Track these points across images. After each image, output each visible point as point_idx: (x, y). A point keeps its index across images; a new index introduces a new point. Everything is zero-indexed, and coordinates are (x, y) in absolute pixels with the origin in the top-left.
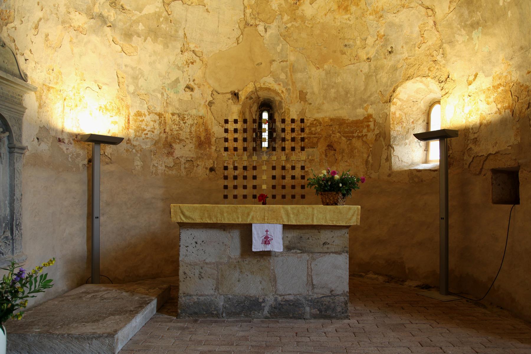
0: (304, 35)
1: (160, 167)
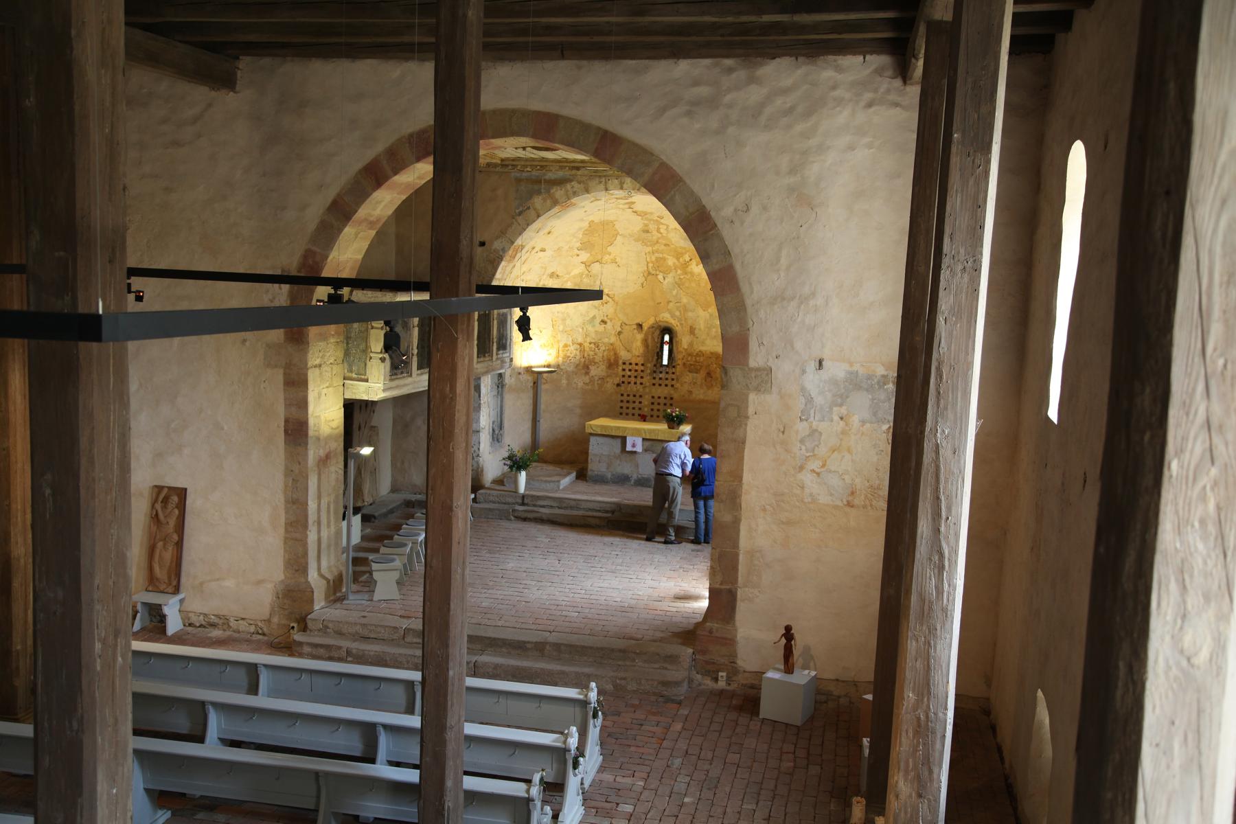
0: (693, 285)
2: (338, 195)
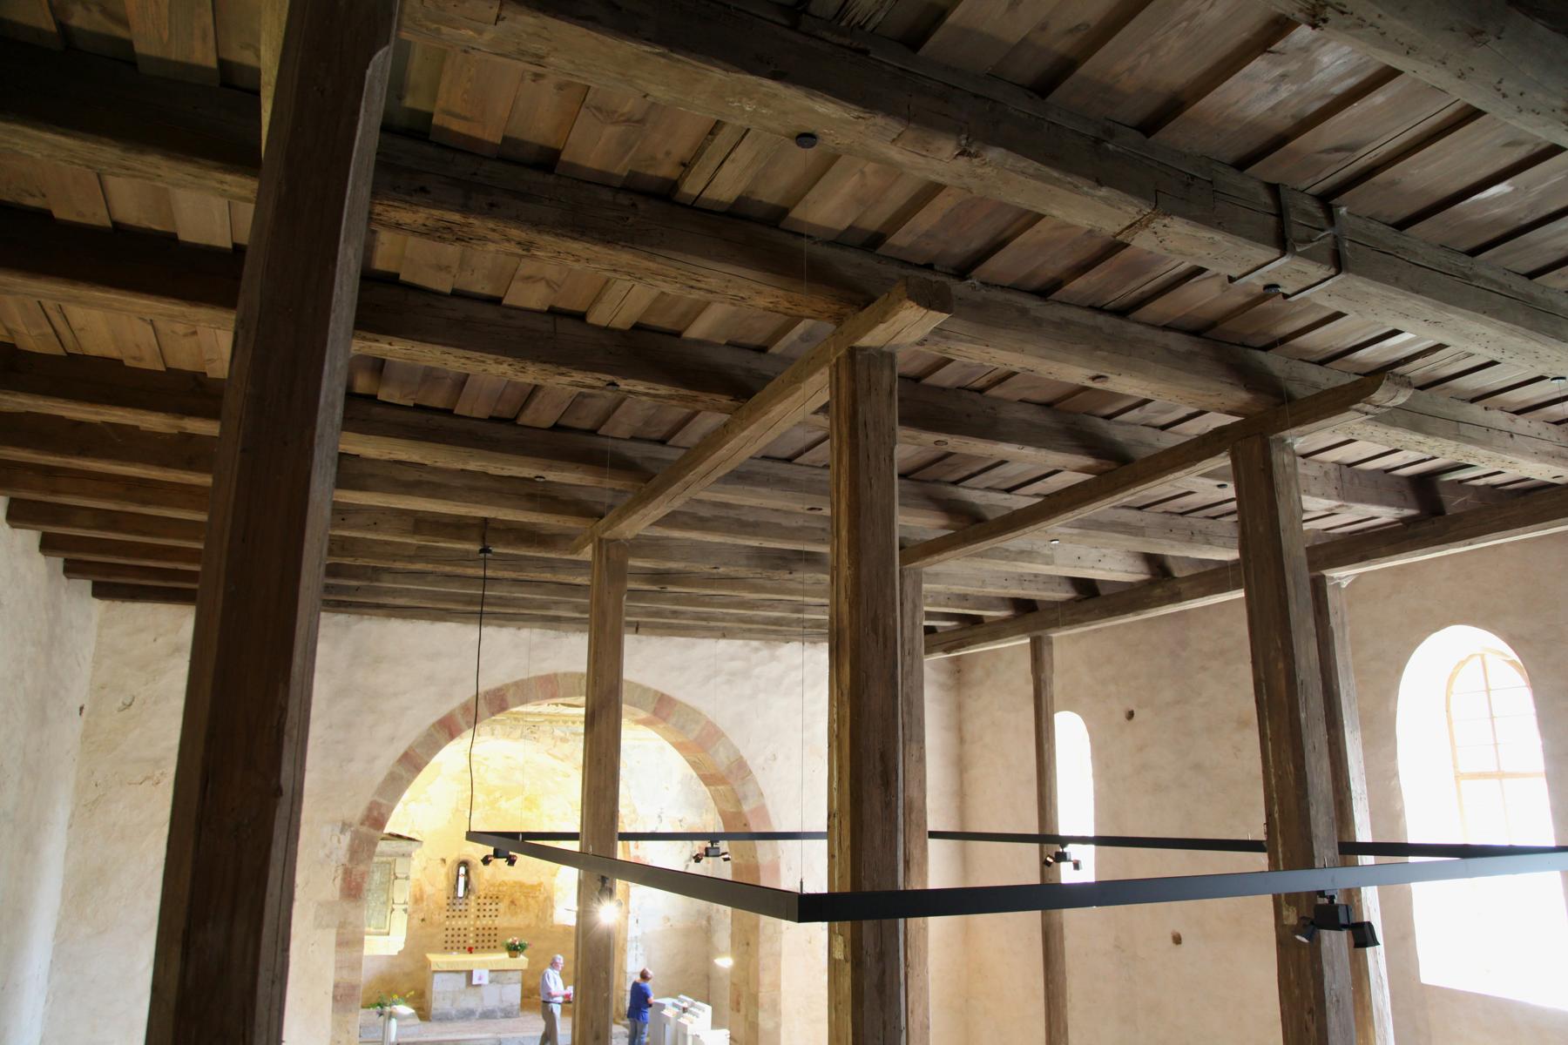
2: (410, 747)
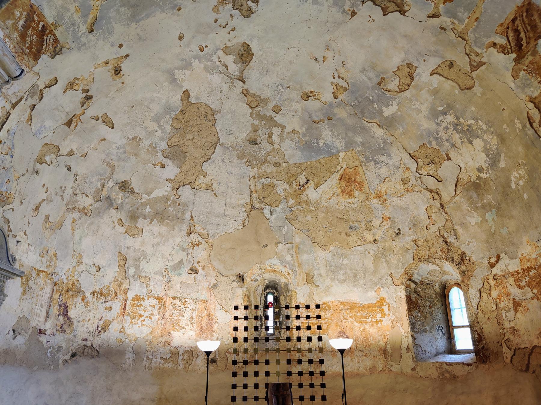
1: (154, 360)
